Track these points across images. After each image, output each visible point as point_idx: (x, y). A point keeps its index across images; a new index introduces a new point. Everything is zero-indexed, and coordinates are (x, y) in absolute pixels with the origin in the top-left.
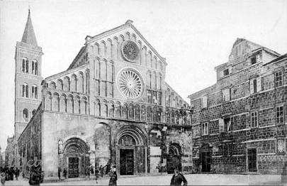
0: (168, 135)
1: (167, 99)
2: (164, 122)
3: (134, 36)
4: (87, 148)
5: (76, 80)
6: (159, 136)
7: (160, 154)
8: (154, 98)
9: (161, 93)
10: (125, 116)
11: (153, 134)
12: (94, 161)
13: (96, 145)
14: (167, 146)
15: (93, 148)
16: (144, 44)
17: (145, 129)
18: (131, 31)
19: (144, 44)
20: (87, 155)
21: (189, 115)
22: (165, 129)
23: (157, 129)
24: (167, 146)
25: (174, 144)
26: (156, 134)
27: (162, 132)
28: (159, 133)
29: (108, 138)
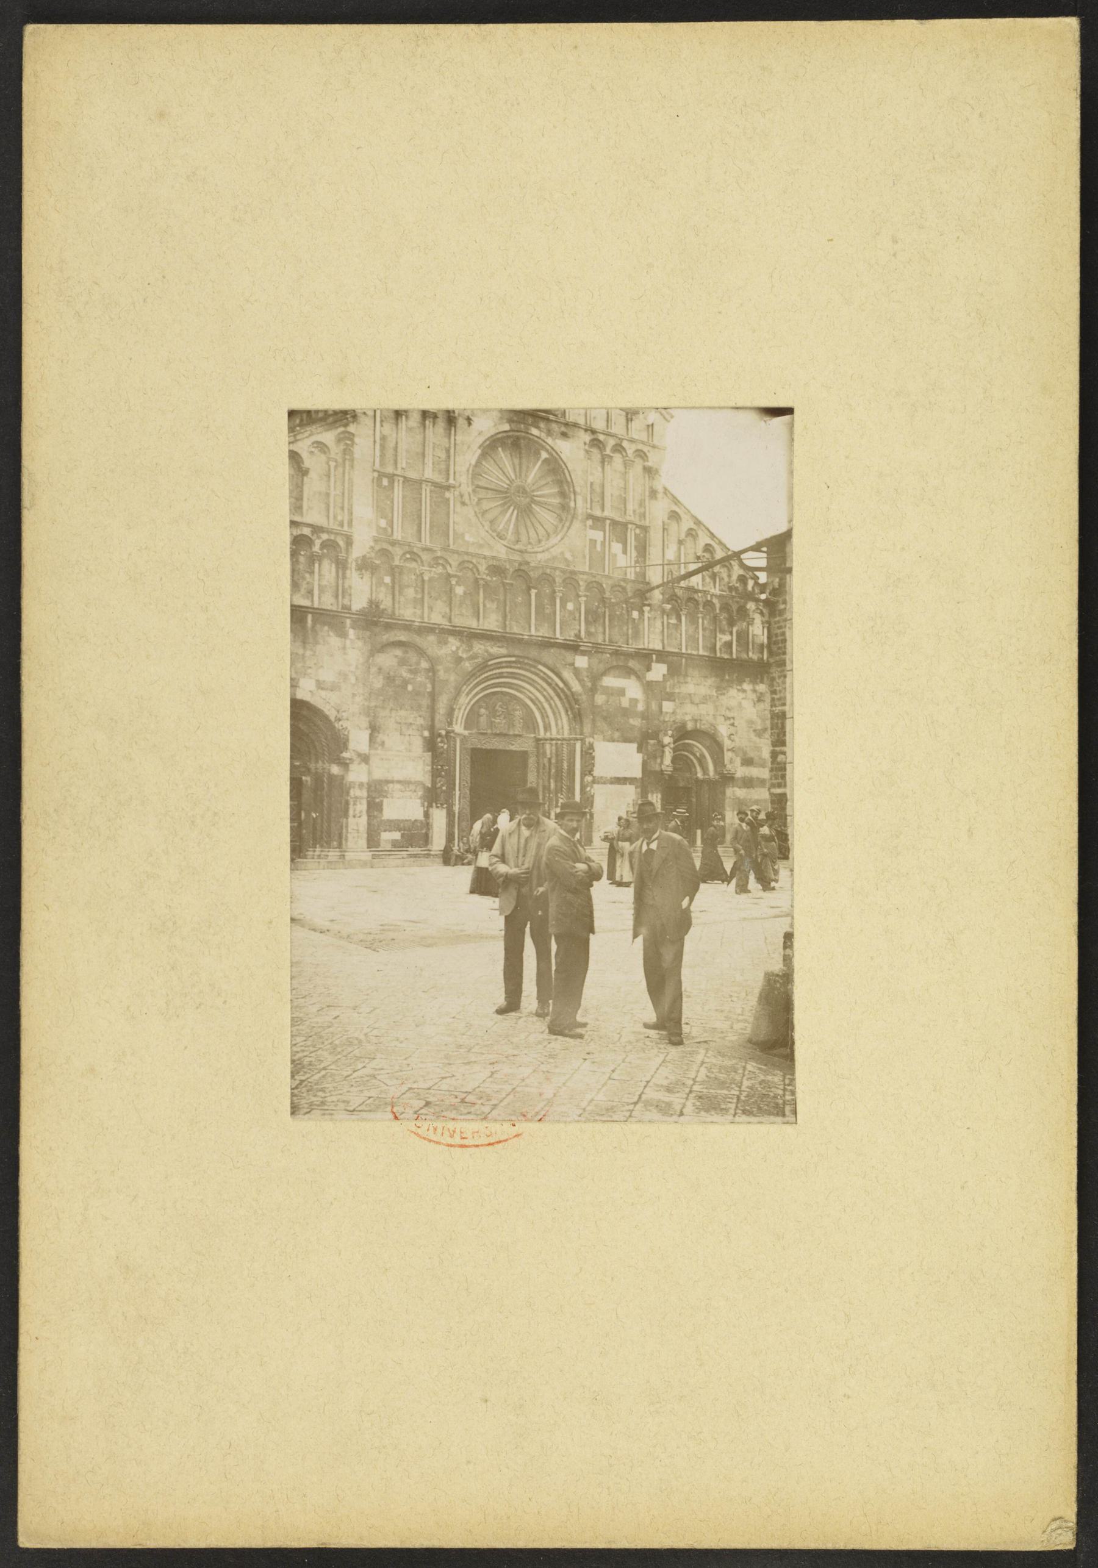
0: (670, 697)
2: (659, 647)
6: (634, 702)
7: (638, 774)
8: (617, 547)
9: (645, 529)
11: (609, 692)
12: (364, 793)
13: (374, 729)
14: (667, 740)
17: (577, 672)
21: (758, 619)
23: (629, 672)
24: (667, 740)
25: (696, 734)
26: (622, 692)
27: (649, 687)
29: (425, 702)
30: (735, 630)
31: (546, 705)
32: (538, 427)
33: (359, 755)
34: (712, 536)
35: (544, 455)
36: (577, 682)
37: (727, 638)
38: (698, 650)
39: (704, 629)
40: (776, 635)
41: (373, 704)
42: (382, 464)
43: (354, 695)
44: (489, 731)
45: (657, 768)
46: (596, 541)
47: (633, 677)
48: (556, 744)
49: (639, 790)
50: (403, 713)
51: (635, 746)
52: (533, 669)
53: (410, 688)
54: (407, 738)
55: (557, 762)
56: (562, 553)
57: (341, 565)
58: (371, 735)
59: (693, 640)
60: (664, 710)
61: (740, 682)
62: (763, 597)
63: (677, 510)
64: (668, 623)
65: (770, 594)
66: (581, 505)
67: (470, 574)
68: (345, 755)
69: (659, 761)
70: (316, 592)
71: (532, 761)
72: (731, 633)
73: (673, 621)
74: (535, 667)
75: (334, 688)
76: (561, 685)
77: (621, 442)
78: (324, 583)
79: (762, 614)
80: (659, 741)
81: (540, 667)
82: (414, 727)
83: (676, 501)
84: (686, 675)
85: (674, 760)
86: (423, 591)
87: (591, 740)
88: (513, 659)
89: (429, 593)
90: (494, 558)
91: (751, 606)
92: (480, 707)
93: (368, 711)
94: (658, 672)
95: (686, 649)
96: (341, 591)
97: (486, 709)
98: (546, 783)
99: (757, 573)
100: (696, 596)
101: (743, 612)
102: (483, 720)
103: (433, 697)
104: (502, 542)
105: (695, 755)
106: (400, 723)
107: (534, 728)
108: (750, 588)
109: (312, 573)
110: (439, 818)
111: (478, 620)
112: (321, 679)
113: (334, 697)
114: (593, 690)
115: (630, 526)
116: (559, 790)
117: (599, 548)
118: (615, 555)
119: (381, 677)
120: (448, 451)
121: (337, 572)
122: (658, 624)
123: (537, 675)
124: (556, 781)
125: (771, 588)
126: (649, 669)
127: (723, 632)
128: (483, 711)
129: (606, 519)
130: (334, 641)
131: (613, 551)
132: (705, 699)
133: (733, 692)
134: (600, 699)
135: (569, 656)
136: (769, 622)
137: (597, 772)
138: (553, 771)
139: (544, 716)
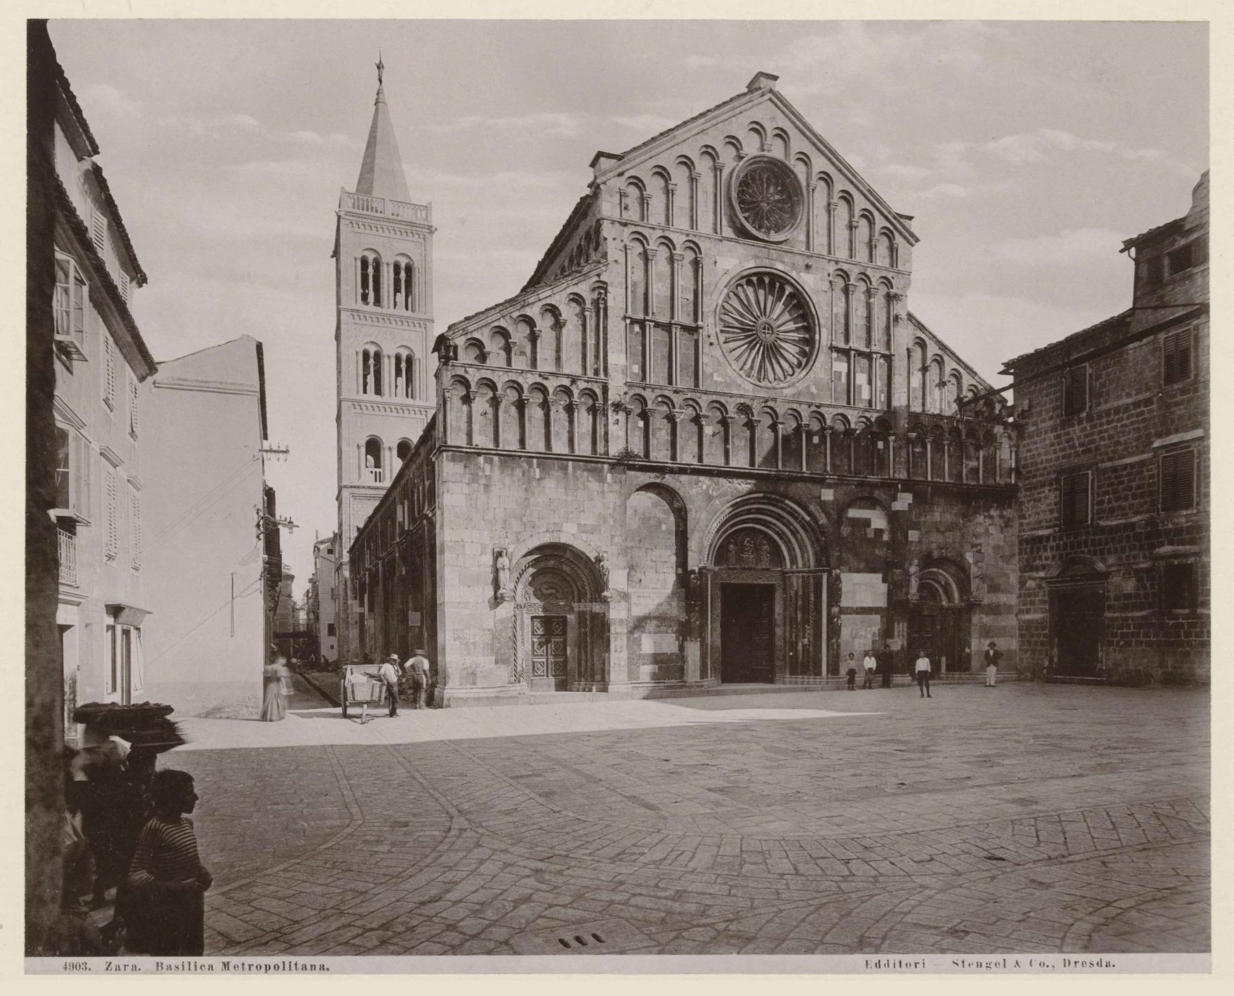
0: (916, 526)
2: (904, 476)
3: (782, 135)
6: (879, 532)
7: (882, 603)
11: (855, 523)
13: (632, 568)
14: (913, 569)
16: (820, 163)
17: (823, 505)
21: (1006, 444)
22: (903, 502)
23: (871, 502)
25: (942, 562)
26: (867, 523)
27: (893, 517)
28: (878, 520)
30: (981, 454)
31: (793, 540)
33: (619, 593)
34: (958, 360)
35: (788, 290)
36: (823, 515)
37: (973, 464)
38: (944, 478)
39: (950, 457)
40: (1026, 459)
41: (629, 545)
42: (634, 310)
43: (612, 537)
44: (738, 566)
45: (904, 597)
46: (841, 373)
47: (878, 507)
48: (803, 577)
49: (885, 620)
50: (657, 552)
51: (880, 576)
54: (662, 575)
55: (804, 593)
58: (628, 574)
59: (937, 469)
60: (910, 539)
61: (988, 508)
62: (1011, 420)
63: (923, 336)
64: (913, 452)
65: (1018, 417)
66: (824, 337)
67: (718, 414)
68: (605, 594)
69: (905, 590)
71: (778, 596)
72: (978, 459)
74: (780, 501)
75: (594, 530)
76: (808, 518)
79: (1010, 437)
80: (904, 569)
81: (787, 502)
82: (669, 565)
83: (922, 327)
84: (932, 504)
85: (921, 587)
87: (838, 571)
88: (761, 495)
90: (741, 396)
91: (998, 429)
92: (730, 543)
93: (625, 551)
94: (903, 502)
95: (932, 477)
97: (735, 544)
98: (793, 615)
99: (1003, 394)
100: (941, 423)
101: (991, 438)
102: (732, 555)
104: (749, 379)
105: (939, 583)
107: (781, 561)
108: (997, 411)
110: (693, 650)
112: (582, 522)
114: (839, 522)
115: (874, 356)
116: (805, 621)
119: (637, 518)
123: (783, 509)
124: (803, 613)
125: (1020, 409)
126: (895, 499)
127: (969, 458)
128: (731, 546)
129: (850, 349)
130: (594, 485)
131: (858, 382)
132: (951, 527)
133: (980, 519)
134: (845, 531)
135: (814, 489)
136: (1018, 447)
137: (845, 602)
138: (800, 603)
139: (791, 549)
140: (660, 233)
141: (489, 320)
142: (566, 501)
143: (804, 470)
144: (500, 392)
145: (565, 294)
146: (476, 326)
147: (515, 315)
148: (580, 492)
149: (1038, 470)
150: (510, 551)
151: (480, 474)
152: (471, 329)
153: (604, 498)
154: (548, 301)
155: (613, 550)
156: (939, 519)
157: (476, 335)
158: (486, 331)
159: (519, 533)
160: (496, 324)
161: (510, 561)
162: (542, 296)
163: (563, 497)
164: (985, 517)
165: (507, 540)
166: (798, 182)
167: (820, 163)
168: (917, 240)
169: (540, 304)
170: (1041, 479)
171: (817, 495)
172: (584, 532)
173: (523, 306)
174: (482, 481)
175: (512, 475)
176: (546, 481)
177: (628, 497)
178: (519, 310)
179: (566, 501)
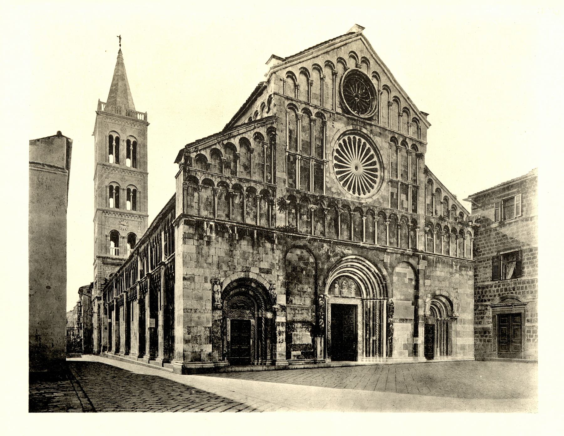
1: (428, 202)
4: (270, 300)
5: (250, 150)
10: (346, 233)
15: (282, 300)
18: (356, 46)
19: (384, 80)
20: (269, 315)
32: (366, 128)
52: (363, 263)
53: (304, 272)
56: (378, 199)
57: (271, 203)
70: (258, 217)
73: (430, 237)
75: (268, 272)
77: (406, 139)
78: (262, 212)
86: (311, 218)
89: (314, 219)
93: (286, 285)
96: (271, 218)
103: (316, 278)
106: (300, 291)
109: (256, 207)
111: (338, 236)
112: (262, 267)
113: (268, 277)
117: (395, 197)
118: (403, 201)
120: (322, 140)
121: (269, 207)
122: (423, 239)
130: (268, 245)
140: (304, 106)
141: (211, 143)
142: (253, 253)
143: (376, 243)
144: (216, 187)
145: (253, 132)
146: (203, 147)
147: (225, 142)
148: (261, 248)
149: (486, 250)
150: (221, 281)
151: (205, 234)
152: (200, 148)
153: (274, 253)
154: (244, 135)
155: (279, 283)
156: (439, 275)
157: (203, 152)
158: (208, 151)
159: (226, 271)
160: (214, 147)
161: (221, 287)
162: (241, 132)
163: (251, 251)
164: (460, 275)
165: (219, 275)
166: (374, 88)
167: (384, 80)
168: (430, 125)
169: (239, 137)
170: (487, 255)
171: (382, 259)
172: (262, 273)
173: (230, 138)
174: (206, 239)
175: (223, 237)
176: (242, 241)
177: (287, 252)
178: (228, 139)
179: (253, 253)
